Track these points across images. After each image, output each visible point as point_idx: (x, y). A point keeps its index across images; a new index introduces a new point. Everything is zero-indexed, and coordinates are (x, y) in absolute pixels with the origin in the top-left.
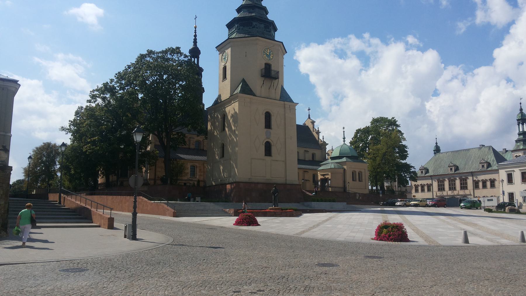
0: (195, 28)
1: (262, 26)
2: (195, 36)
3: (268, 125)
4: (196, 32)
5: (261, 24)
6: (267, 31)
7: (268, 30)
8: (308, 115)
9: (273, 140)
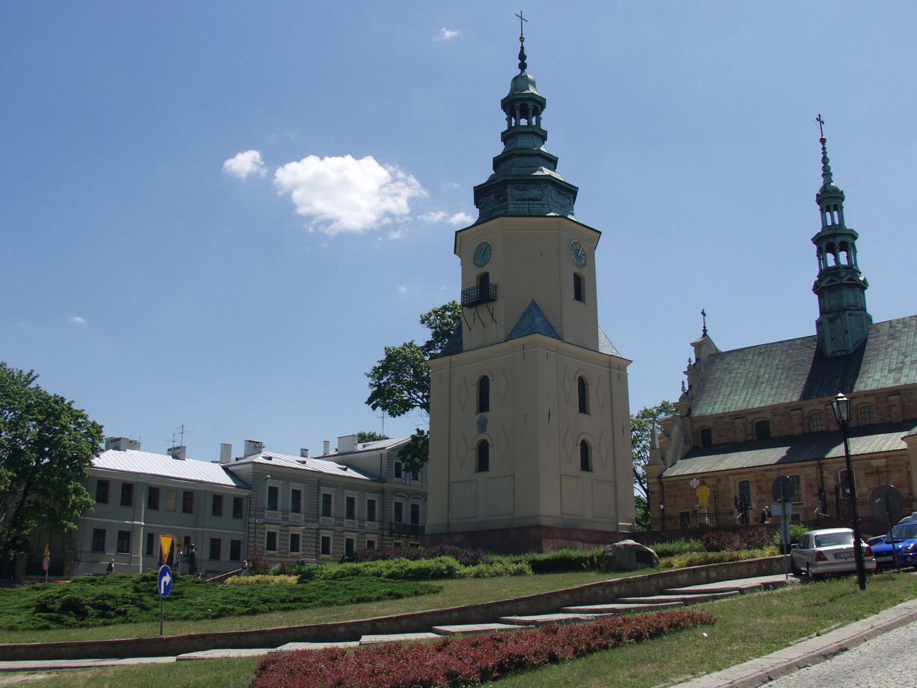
0: (823, 141)
1: (492, 197)
2: (825, 160)
3: (483, 405)
4: (826, 153)
6: (501, 202)
7: (502, 198)
8: (703, 329)
9: (493, 435)
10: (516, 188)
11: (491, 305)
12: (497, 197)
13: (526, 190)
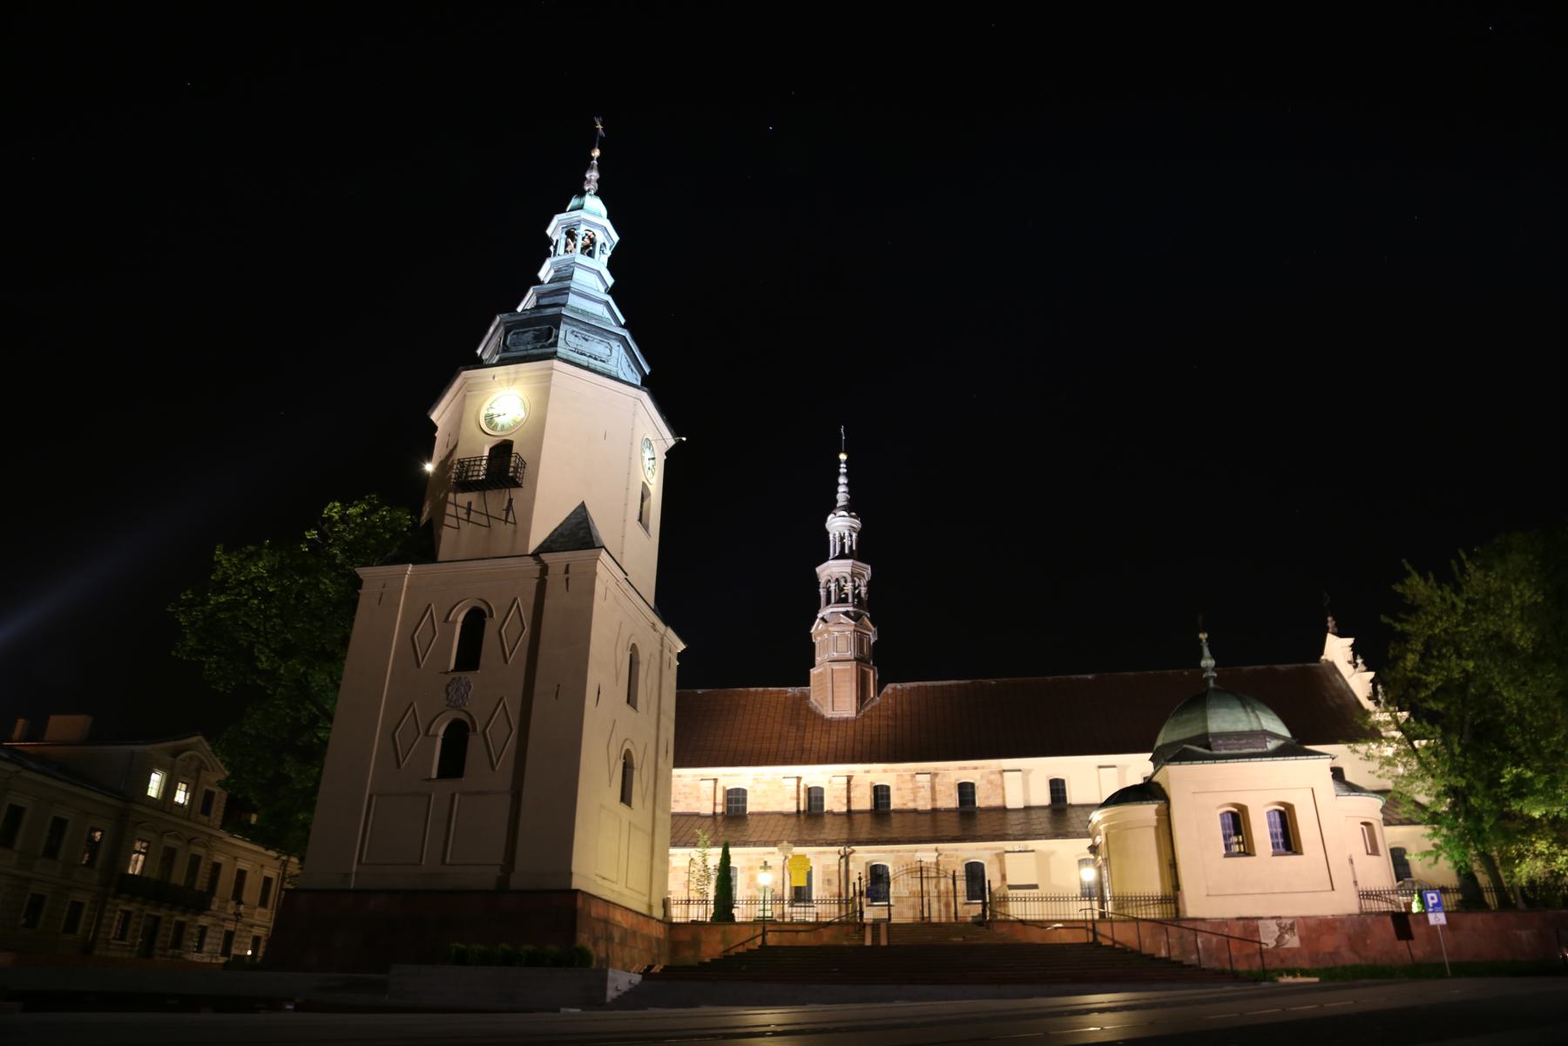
1: (529, 336)
5: (526, 332)
10: (573, 332)
11: (515, 493)
12: (537, 338)
13: (587, 340)
